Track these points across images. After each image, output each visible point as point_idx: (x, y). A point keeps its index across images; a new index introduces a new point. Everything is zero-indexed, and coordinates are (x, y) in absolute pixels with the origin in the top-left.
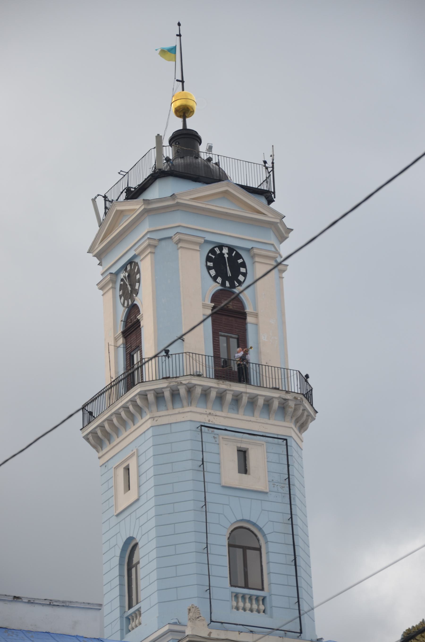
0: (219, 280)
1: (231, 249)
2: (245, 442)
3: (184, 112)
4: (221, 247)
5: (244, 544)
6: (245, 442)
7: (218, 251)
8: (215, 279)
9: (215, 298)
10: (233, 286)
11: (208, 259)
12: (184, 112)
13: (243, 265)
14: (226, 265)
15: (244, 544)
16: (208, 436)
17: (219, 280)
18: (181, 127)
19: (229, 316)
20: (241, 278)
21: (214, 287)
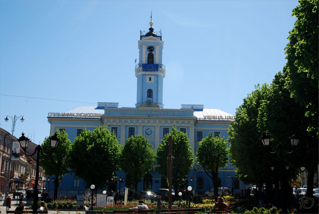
0: (149, 51)
1: (152, 46)
2: (150, 76)
3: (151, 25)
4: (150, 46)
5: (150, 92)
6: (150, 76)
7: (149, 47)
8: (148, 51)
9: (149, 55)
10: (152, 52)
11: (148, 48)
12: (151, 25)
13: (154, 48)
14: (151, 49)
15: (150, 92)
16: (144, 76)
17: (149, 51)
18: (151, 27)
19: (151, 57)
20: (153, 50)
21: (149, 52)
